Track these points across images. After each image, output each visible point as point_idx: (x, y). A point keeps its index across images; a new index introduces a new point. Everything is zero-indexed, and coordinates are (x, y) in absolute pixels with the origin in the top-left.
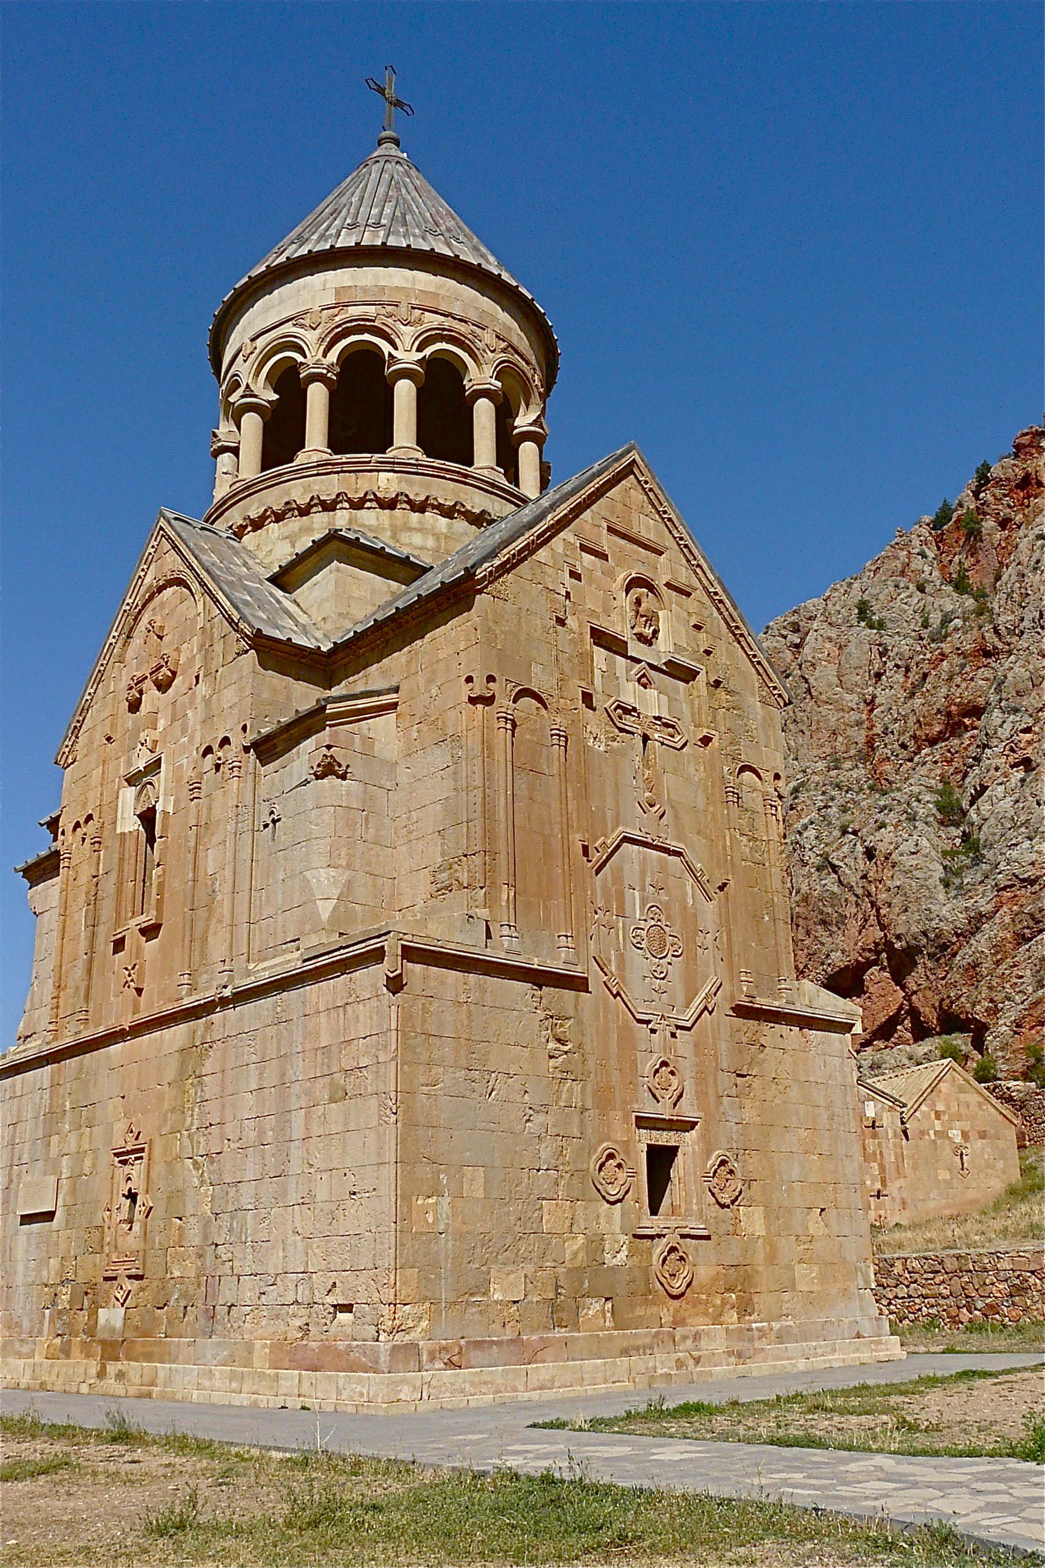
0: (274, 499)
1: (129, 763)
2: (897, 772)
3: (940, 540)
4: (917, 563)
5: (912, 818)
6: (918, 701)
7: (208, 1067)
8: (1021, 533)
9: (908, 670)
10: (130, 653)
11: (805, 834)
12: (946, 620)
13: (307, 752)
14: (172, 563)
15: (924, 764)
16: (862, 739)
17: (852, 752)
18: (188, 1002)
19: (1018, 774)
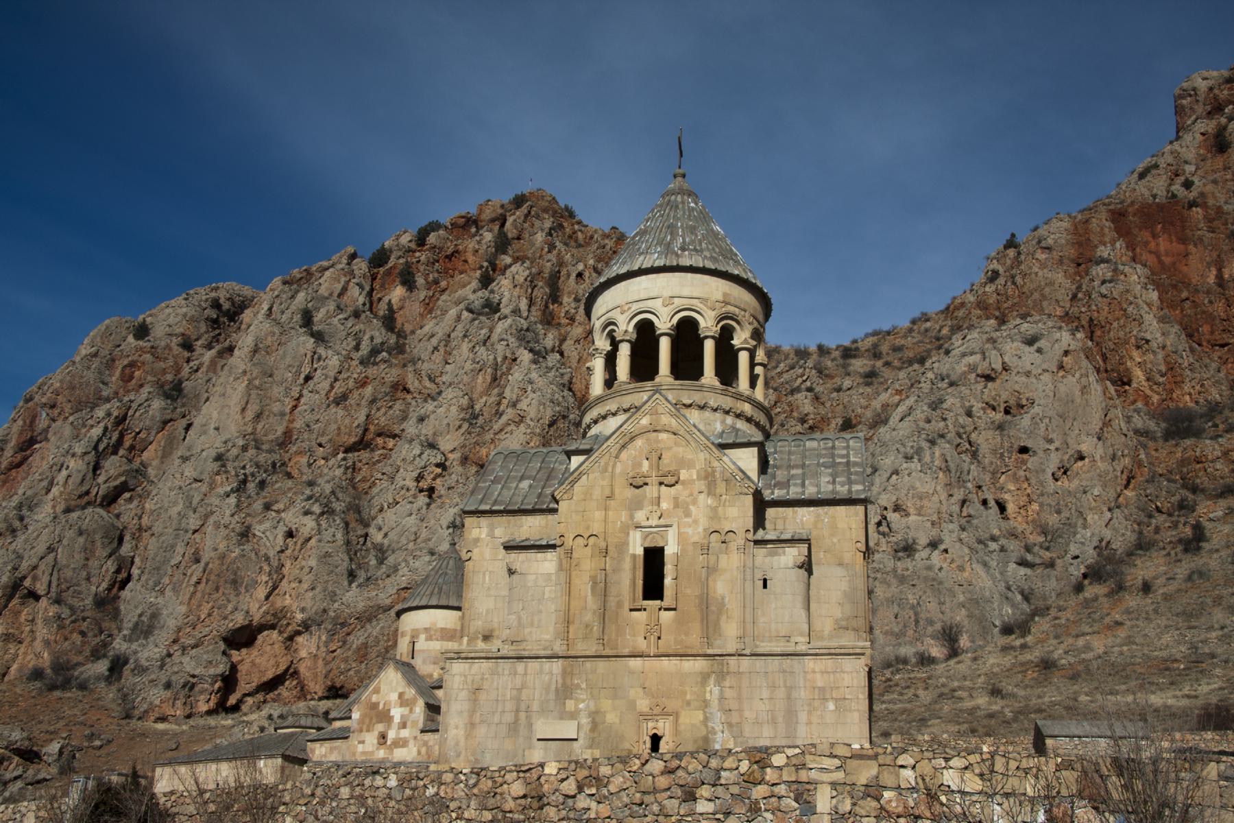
0: (697, 397)
1: (632, 517)
2: (310, 465)
3: (374, 278)
4: (354, 291)
5: (332, 512)
6: (341, 412)
7: (727, 683)
8: (444, 297)
9: (336, 380)
10: (624, 455)
11: (227, 500)
12: (375, 352)
13: (793, 555)
14: (666, 420)
15: (340, 466)
16: (280, 430)
17: (271, 437)
18: (710, 651)
19: (422, 499)
